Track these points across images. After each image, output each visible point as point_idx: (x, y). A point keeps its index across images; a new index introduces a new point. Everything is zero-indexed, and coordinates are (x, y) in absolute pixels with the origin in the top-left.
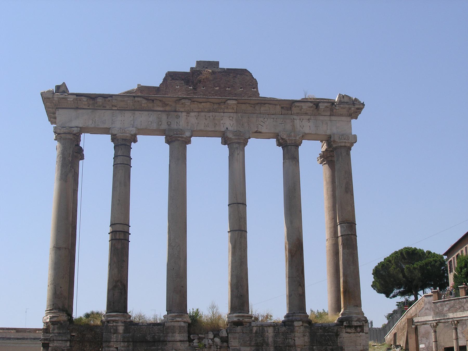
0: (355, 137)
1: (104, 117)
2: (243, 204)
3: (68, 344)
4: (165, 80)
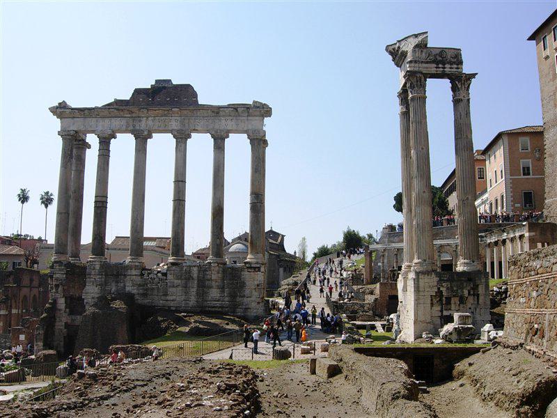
0: (265, 132)
1: (92, 122)
2: (182, 181)
3: (65, 276)
4: (133, 94)
